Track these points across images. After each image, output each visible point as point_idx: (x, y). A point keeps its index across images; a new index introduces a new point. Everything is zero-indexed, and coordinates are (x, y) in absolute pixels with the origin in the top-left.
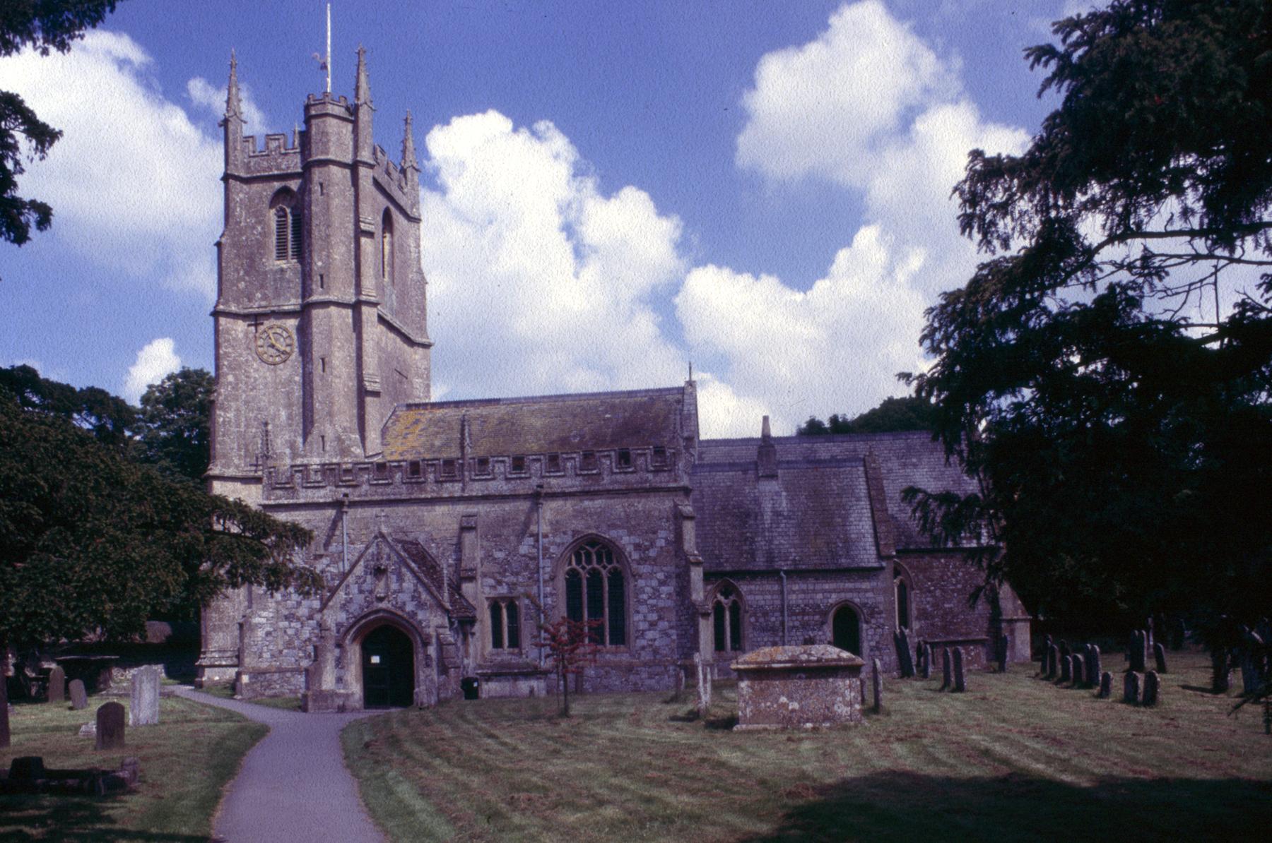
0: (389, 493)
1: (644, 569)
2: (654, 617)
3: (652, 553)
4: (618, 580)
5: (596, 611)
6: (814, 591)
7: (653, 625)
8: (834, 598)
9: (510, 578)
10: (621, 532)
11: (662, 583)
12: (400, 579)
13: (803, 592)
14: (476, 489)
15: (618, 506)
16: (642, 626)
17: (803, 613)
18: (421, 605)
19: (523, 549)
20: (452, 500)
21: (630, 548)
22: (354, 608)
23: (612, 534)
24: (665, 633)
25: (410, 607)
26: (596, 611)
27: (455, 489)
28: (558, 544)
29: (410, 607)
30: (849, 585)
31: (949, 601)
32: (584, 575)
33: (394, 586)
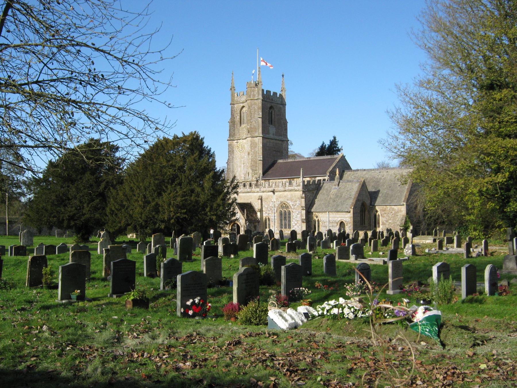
0: (246, 190)
1: (294, 211)
2: (296, 222)
3: (296, 207)
4: (290, 214)
6: (335, 217)
8: (339, 219)
9: (268, 212)
11: (298, 214)
13: (333, 217)
16: (294, 225)
17: (332, 223)
19: (271, 205)
20: (257, 192)
23: (288, 202)
24: (298, 226)
27: (258, 189)
28: (277, 204)
30: (343, 216)
31: (390, 220)
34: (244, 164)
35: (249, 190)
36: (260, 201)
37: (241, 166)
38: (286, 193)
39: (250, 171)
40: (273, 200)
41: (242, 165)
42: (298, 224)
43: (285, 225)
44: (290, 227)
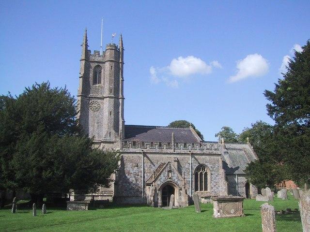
3: (214, 169)
5: (201, 182)
7: (215, 186)
10: (208, 164)
11: (217, 176)
12: (174, 173)
14: (177, 151)
15: (208, 157)
16: (213, 186)
18: (179, 180)
19: (187, 167)
20: (171, 154)
21: (210, 168)
22: (162, 180)
23: (206, 164)
25: (176, 180)
26: (201, 182)
29: (176, 180)
32: (199, 173)
33: (173, 175)
34: (98, 123)
35: (158, 150)
36: (176, 163)
37: (94, 126)
38: (204, 157)
39: (113, 132)
40: (189, 162)
41: (96, 124)
42: (217, 186)
43: (201, 185)
44: (206, 189)
